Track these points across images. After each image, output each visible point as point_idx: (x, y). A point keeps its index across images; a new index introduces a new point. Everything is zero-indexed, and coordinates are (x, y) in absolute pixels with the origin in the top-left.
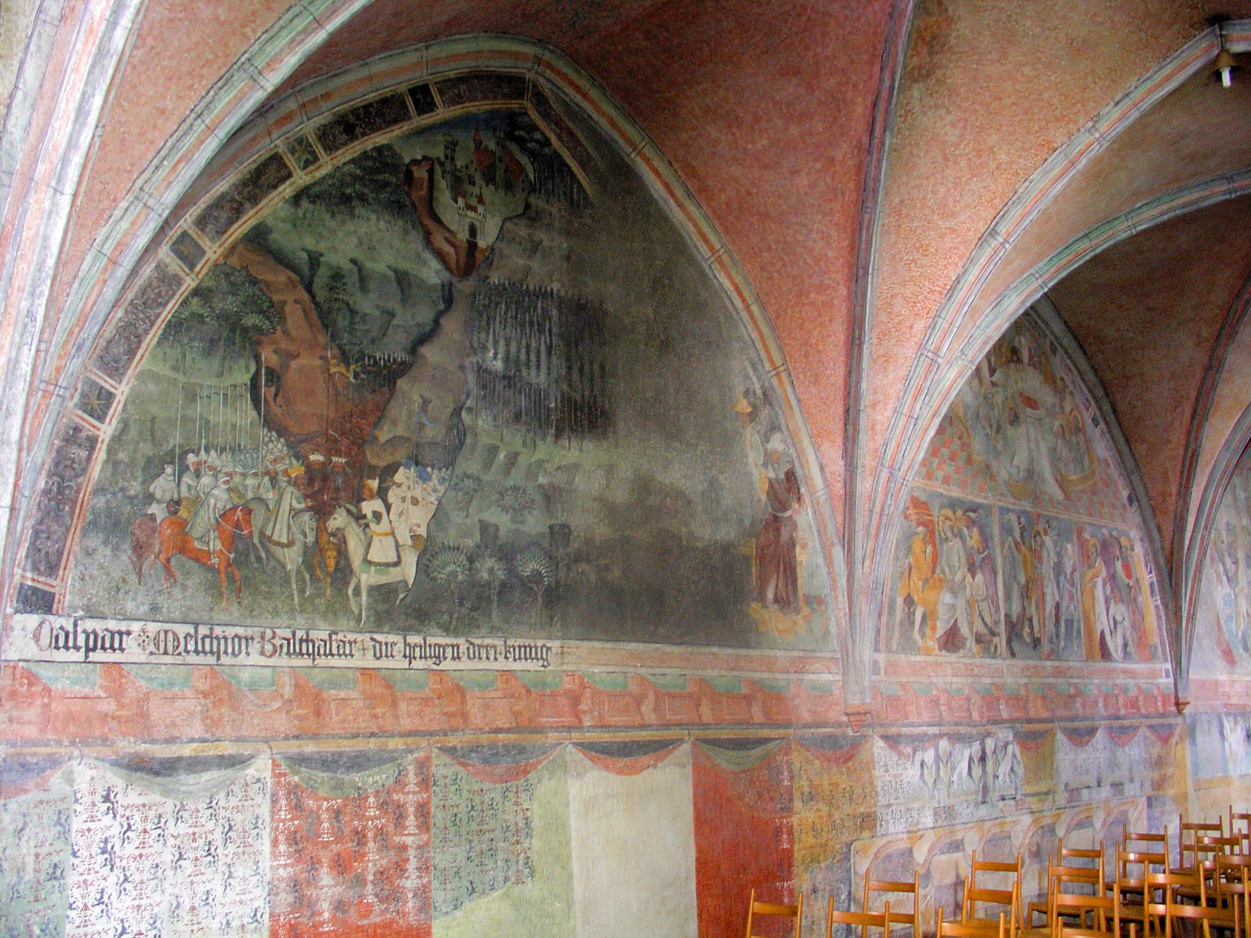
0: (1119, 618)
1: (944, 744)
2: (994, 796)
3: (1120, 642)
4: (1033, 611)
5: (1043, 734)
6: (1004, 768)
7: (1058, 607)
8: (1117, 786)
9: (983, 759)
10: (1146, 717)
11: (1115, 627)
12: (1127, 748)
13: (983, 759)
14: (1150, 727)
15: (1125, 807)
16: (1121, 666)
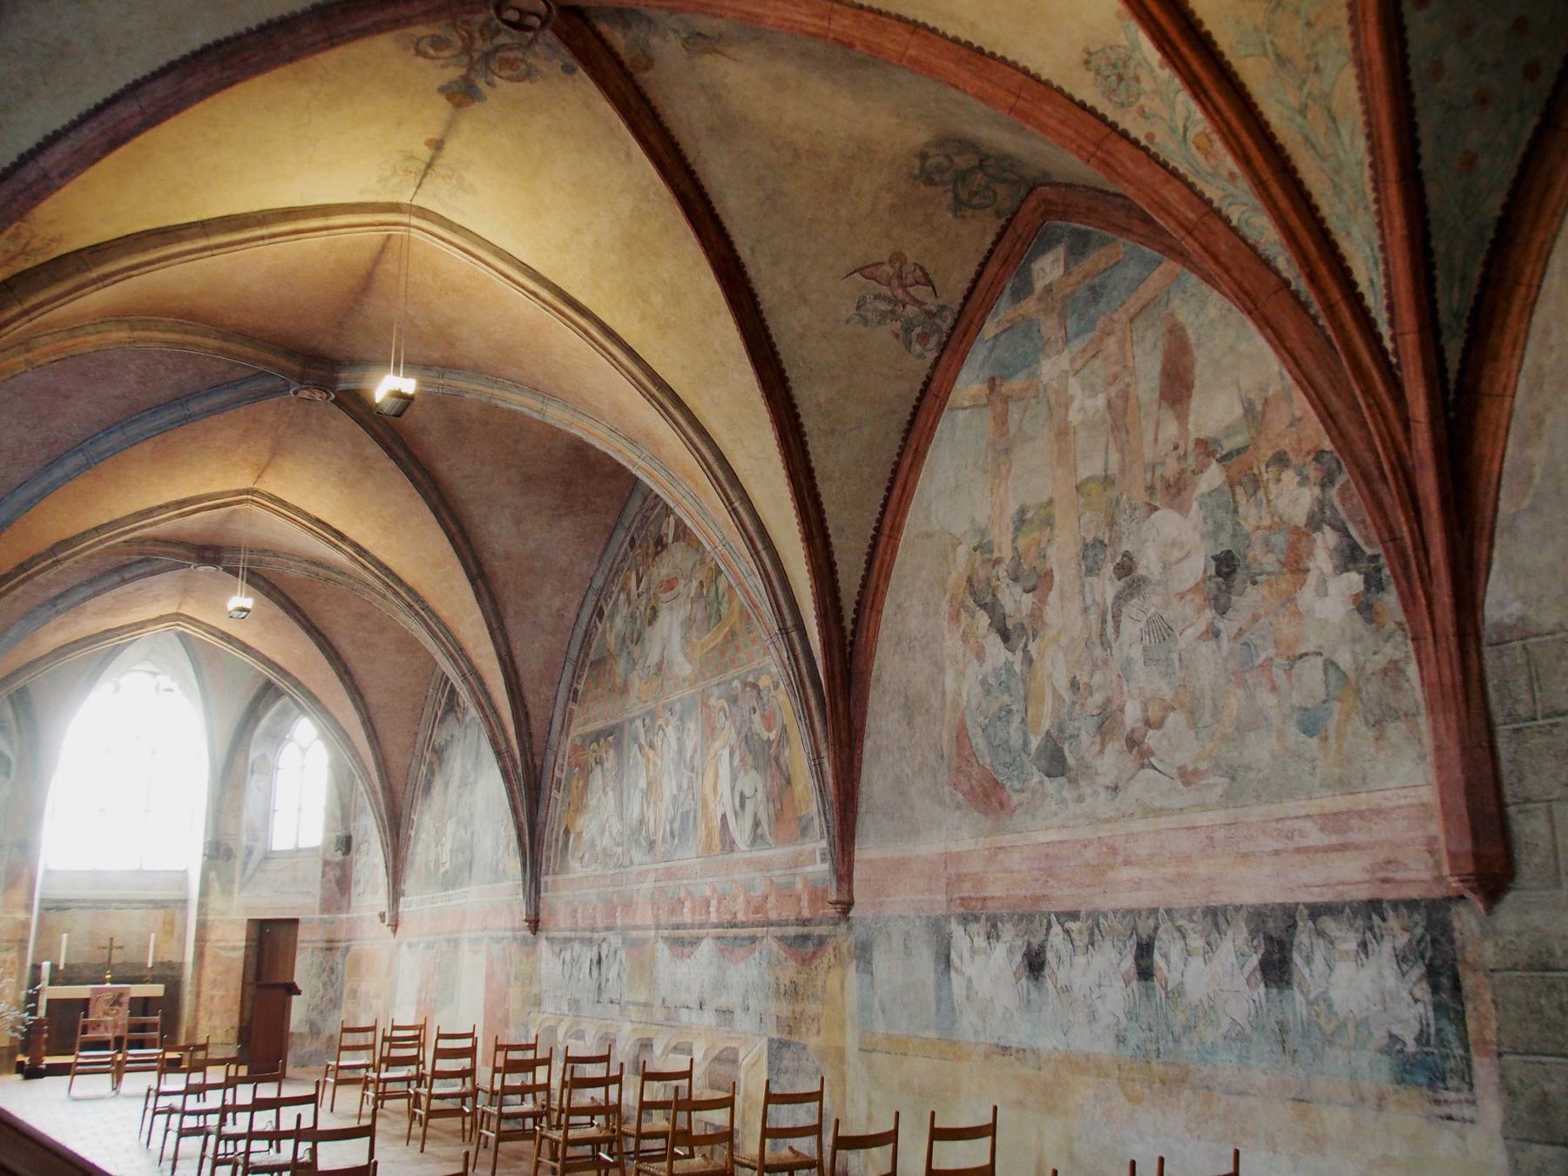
0: (748, 792)
1: (577, 946)
2: (605, 997)
3: (748, 823)
4: (650, 816)
5: (644, 941)
6: (613, 974)
7: (675, 798)
8: (725, 1013)
9: (599, 961)
10: (779, 924)
11: (742, 805)
12: (742, 965)
13: (599, 961)
14: (781, 939)
15: (734, 1045)
16: (748, 855)
